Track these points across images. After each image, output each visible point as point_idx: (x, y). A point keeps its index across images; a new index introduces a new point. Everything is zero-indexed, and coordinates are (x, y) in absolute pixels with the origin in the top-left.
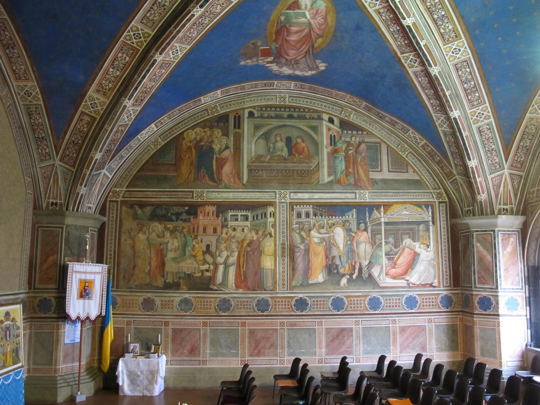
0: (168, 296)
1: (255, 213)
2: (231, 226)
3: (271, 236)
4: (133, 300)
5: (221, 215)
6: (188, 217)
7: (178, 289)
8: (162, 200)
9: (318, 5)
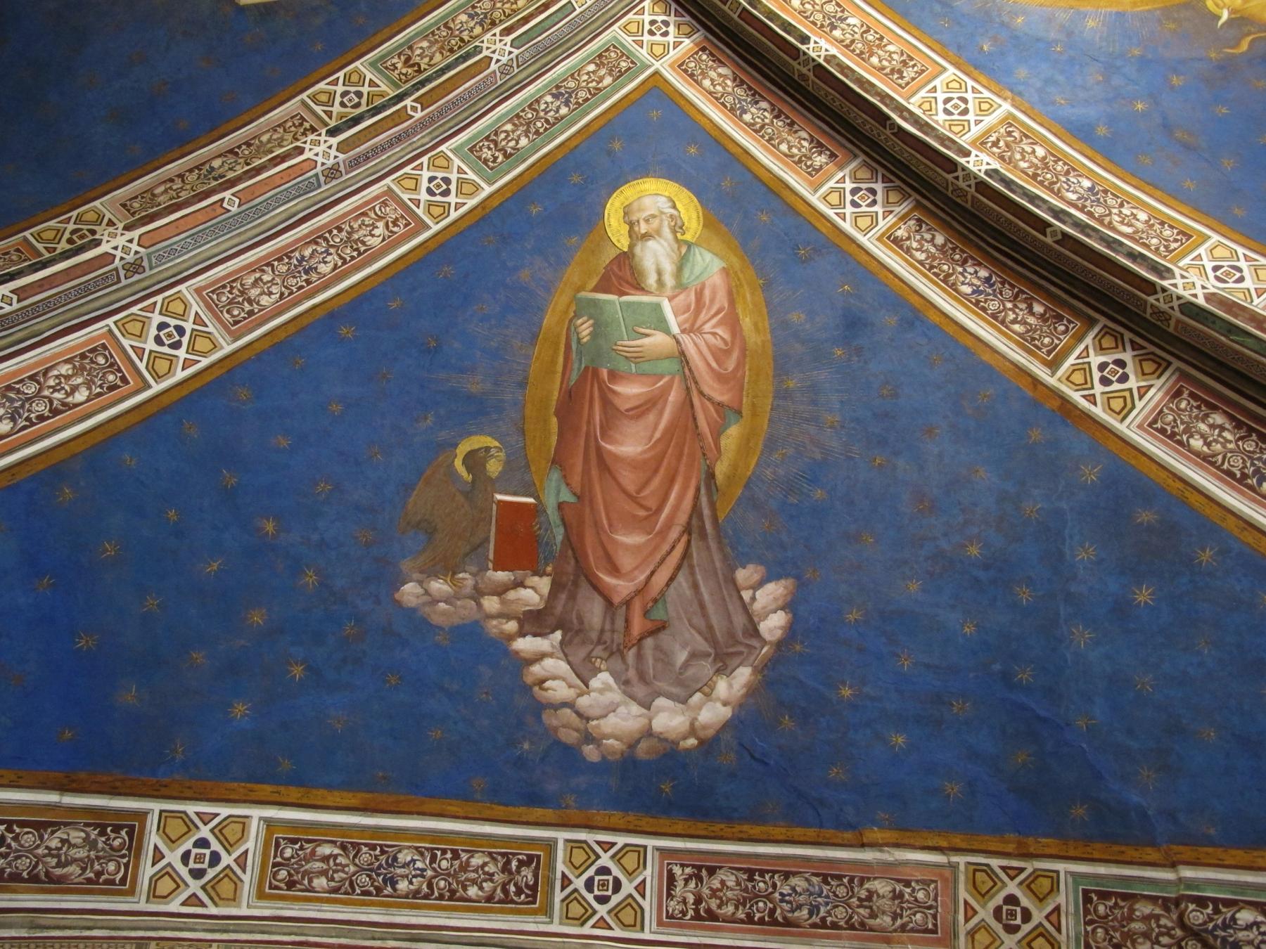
9: (697, 271)
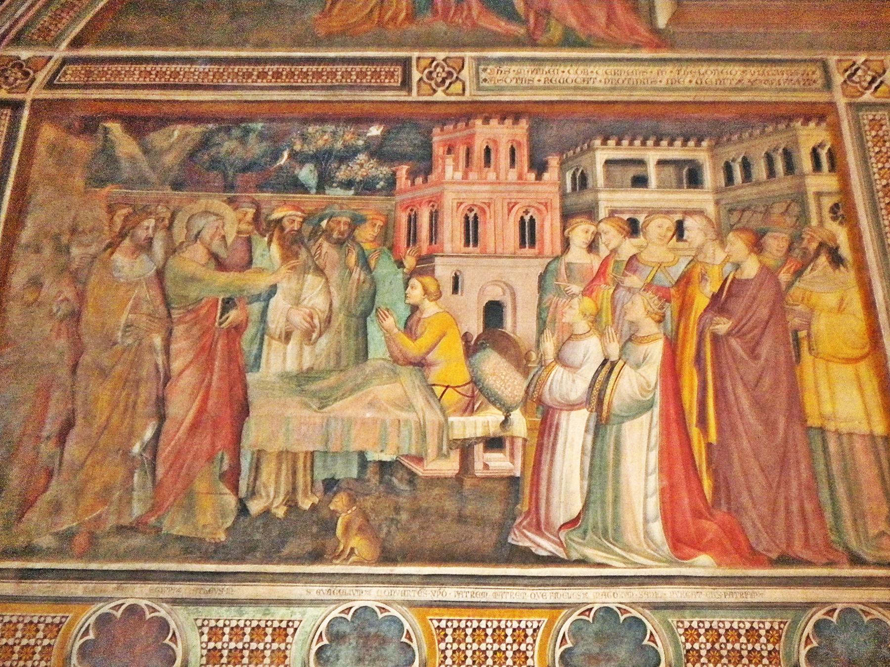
0: (255, 602)
1: (733, 152)
2: (613, 213)
3: (836, 260)
4: (32, 627)
5: (554, 161)
6: (385, 170)
7: (317, 557)
8: (250, 96)
